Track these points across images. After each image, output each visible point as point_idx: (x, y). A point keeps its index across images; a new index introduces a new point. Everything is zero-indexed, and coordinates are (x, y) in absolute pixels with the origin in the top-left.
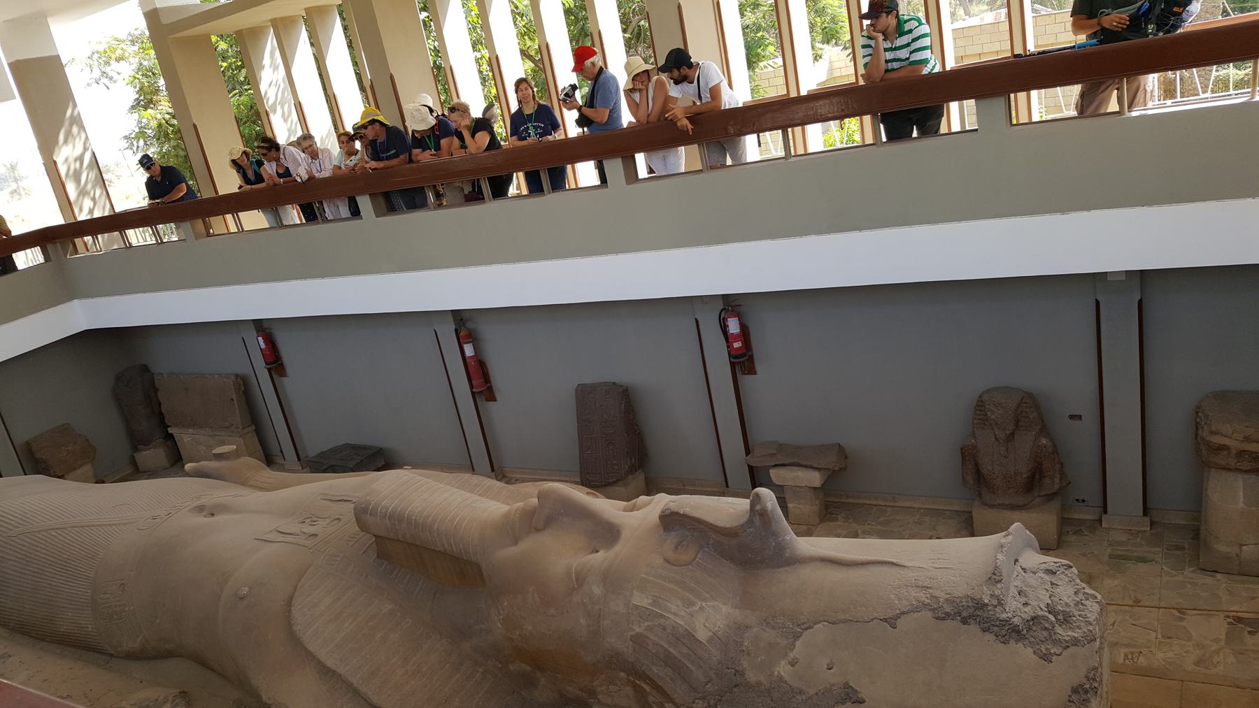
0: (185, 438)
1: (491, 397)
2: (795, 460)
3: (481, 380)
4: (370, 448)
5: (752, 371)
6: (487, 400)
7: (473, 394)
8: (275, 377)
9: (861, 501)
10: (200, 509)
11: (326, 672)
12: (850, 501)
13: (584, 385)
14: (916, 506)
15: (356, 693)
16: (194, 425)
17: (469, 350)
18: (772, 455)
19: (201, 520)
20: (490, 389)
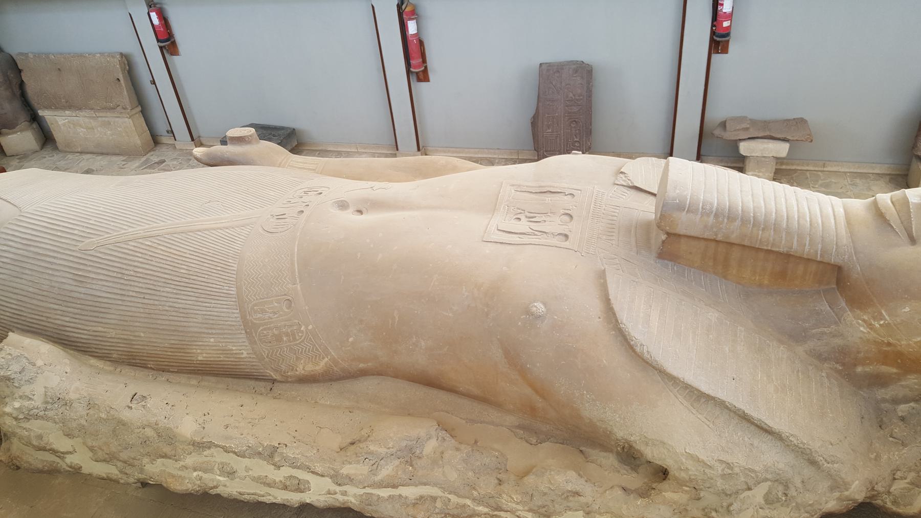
0: (59, 121)
1: (424, 76)
2: (767, 133)
3: (415, 57)
4: (282, 128)
5: (725, 50)
6: (419, 80)
7: (408, 72)
8: (167, 55)
9: (793, 167)
10: (343, 205)
11: (698, 397)
12: (784, 167)
13: (550, 65)
14: (843, 170)
15: (745, 418)
16: (70, 105)
17: (412, 27)
18: (747, 129)
19: (349, 217)
20: (425, 71)
